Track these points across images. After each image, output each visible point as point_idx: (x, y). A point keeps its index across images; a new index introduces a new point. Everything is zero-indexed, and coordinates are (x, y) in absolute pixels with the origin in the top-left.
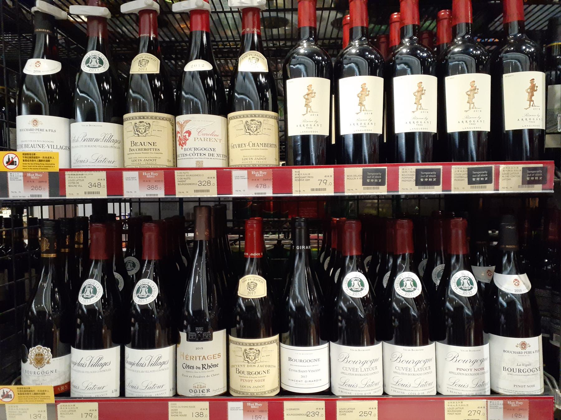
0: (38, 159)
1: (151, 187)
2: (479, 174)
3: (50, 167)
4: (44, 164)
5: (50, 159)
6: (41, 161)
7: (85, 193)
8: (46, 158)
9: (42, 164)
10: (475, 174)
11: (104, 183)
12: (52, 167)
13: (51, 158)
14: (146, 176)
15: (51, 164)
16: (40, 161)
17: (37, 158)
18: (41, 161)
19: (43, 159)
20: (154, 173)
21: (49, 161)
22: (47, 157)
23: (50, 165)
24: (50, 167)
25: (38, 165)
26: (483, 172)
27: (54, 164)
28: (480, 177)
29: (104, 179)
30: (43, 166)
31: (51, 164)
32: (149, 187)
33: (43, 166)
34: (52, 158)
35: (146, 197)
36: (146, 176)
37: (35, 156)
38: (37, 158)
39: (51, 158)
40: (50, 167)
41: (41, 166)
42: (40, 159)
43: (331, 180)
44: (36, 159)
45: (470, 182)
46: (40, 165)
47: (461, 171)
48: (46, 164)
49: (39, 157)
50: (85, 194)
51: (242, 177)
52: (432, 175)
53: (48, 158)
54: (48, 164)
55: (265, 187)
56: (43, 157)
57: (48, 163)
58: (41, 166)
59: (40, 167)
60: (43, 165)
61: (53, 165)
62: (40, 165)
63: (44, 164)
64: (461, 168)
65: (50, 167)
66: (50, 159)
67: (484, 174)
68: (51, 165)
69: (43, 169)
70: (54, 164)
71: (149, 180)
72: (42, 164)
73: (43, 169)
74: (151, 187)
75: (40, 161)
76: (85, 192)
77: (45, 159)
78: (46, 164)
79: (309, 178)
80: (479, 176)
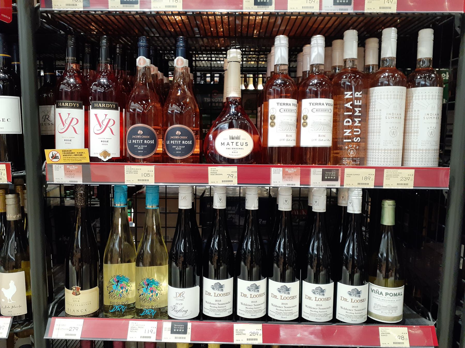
0: (74, 154)
5: (82, 154)
8: (79, 153)
12: (85, 159)
13: (83, 153)
16: (75, 155)
17: (73, 153)
19: (78, 154)
21: (82, 155)
22: (80, 152)
25: (74, 158)
37: (71, 152)
38: (73, 153)
39: (83, 153)
44: (72, 154)
49: (74, 153)
53: (81, 153)
56: (77, 153)
57: (81, 156)
60: (78, 158)
61: (85, 158)
62: (76, 158)
68: (84, 158)
75: (75, 155)
77: (79, 154)
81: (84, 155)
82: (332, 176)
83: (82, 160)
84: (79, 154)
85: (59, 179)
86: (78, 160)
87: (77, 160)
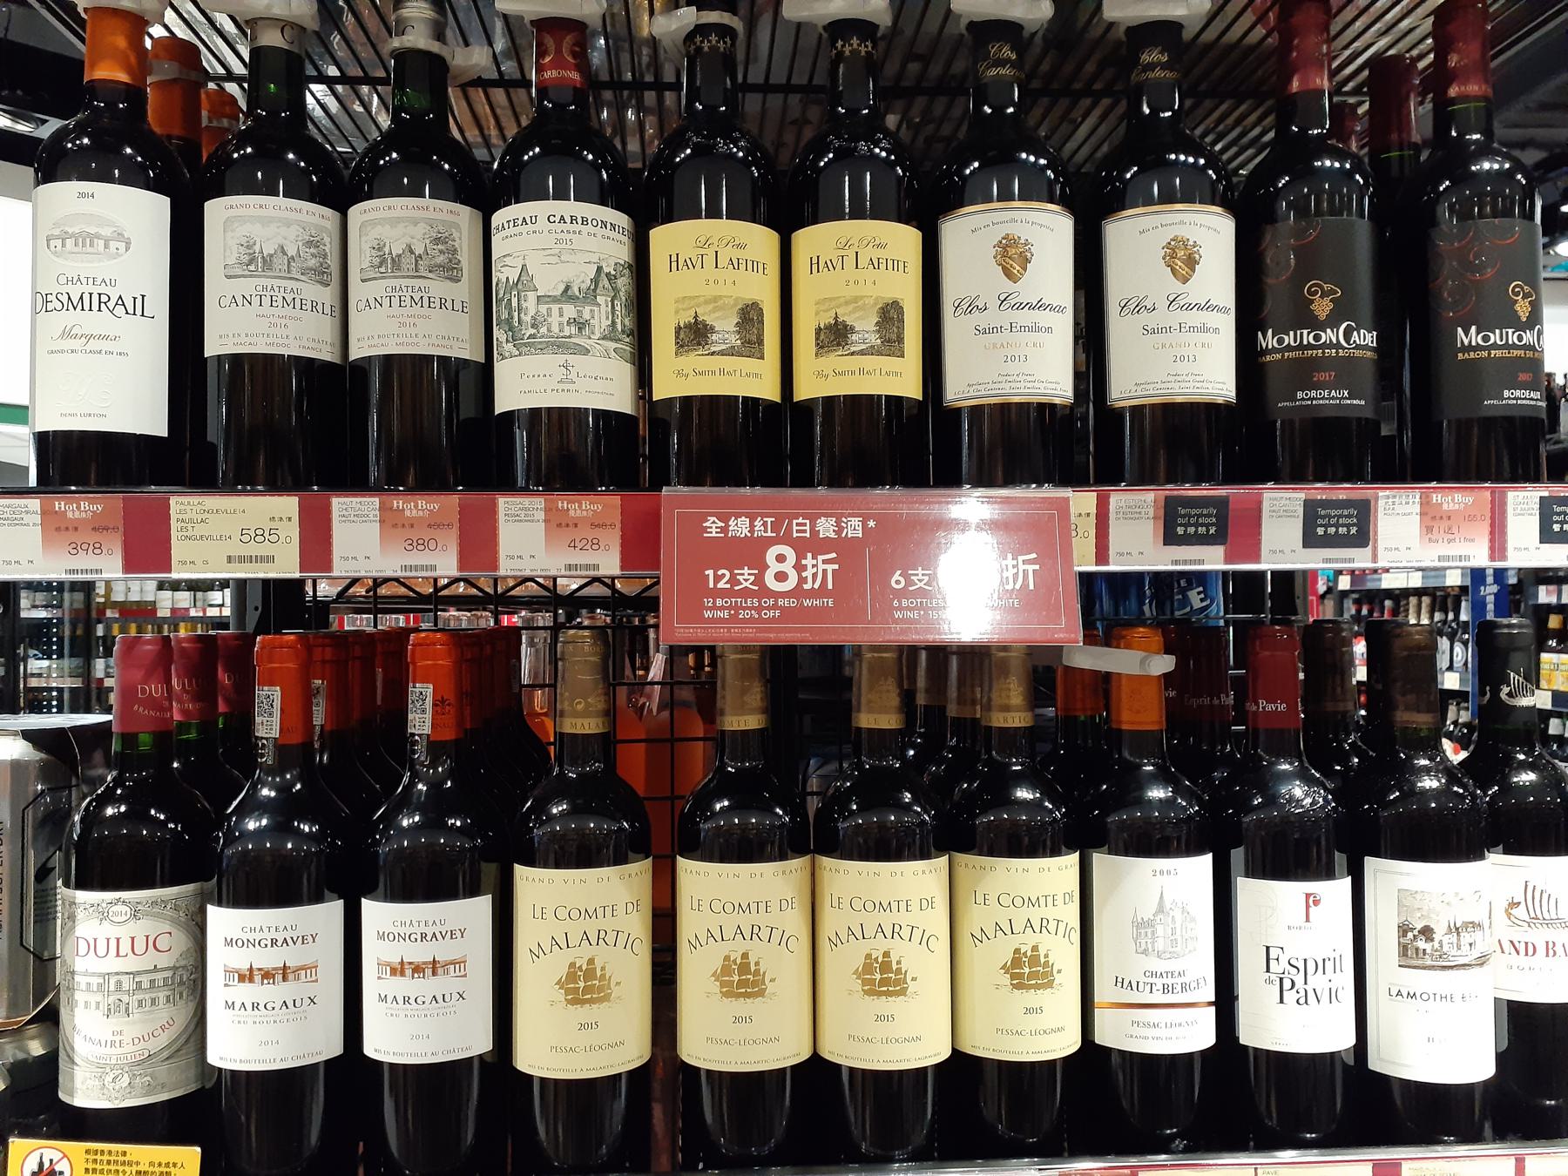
1: (415, 544)
2: (1334, 517)
7: (230, 560)
10: (1183, 516)
14: (403, 510)
26: (1346, 512)
28: (1197, 525)
32: (410, 542)
43: (292, 531)
45: (1170, 538)
52: (1205, 516)
55: (595, 547)
67: (1349, 516)
74: (415, 544)
79: (215, 526)
80: (1333, 521)
82: (1343, 525)
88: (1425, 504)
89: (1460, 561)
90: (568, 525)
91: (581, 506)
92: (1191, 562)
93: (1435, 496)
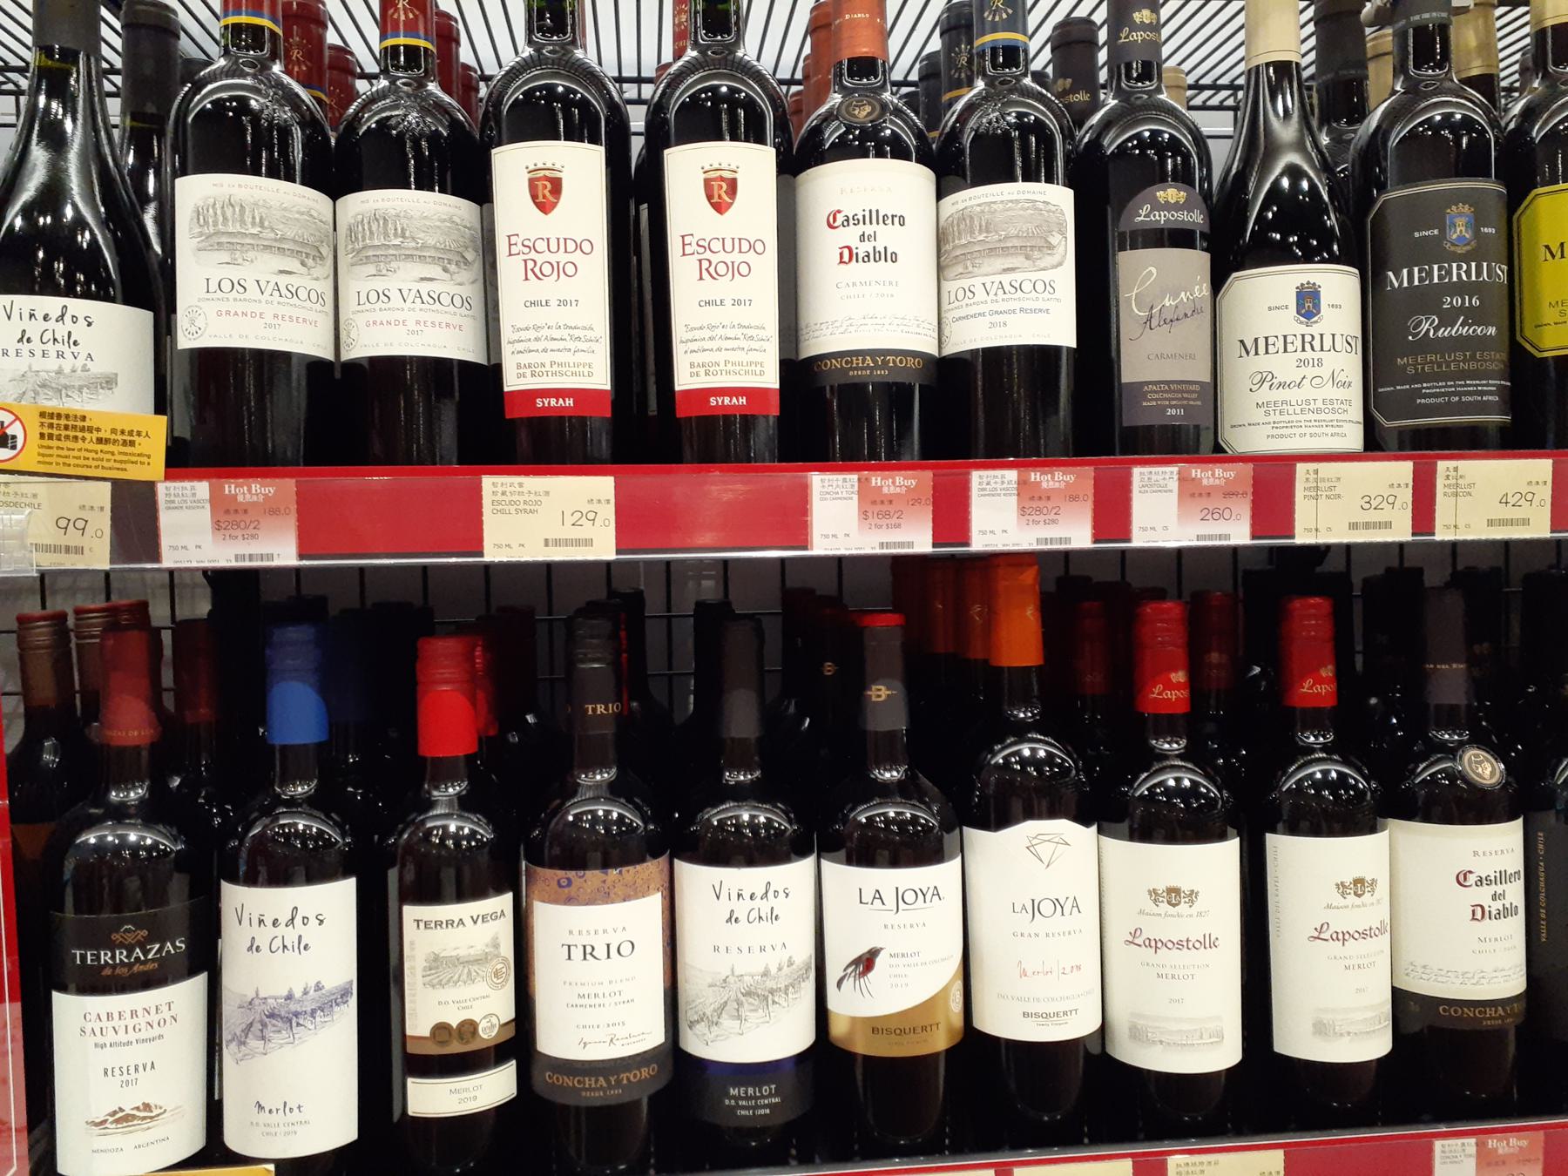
3: (133, 463)
4: (113, 454)
5: (136, 438)
6: (107, 441)
9: (107, 452)
11: (608, 513)
13: (139, 434)
15: (139, 455)
16: (100, 441)
18: (107, 441)
19: (113, 437)
20: (1224, 470)
21: (132, 443)
22: (127, 429)
23: (134, 459)
24: (136, 463)
27: (149, 457)
29: (608, 502)
30: (108, 460)
31: (139, 455)
33: (108, 460)
34: (144, 434)
35: (234, 564)
36: (1201, 479)
39: (139, 434)
40: (136, 463)
41: (102, 460)
42: (101, 435)
46: (100, 455)
47: (504, 493)
48: (120, 453)
49: (98, 430)
50: (547, 545)
51: (196, 504)
53: (131, 433)
54: (126, 454)
56: (114, 431)
57: (128, 449)
58: (102, 460)
59: (99, 463)
60: (109, 456)
61: (145, 459)
62: (100, 455)
63: (113, 454)
64: (521, 485)
65: (133, 463)
66: (136, 438)
68: (139, 459)
69: (110, 469)
70: (149, 457)
71: (1208, 493)
72: (107, 452)
73: (110, 469)
75: (100, 441)
76: (546, 540)
77: (120, 437)
78: (120, 453)
81: (143, 446)
83: (128, 466)
84: (120, 437)
85: (508, 546)
86: (111, 464)
87: (105, 464)
88: (1183, 480)
89: (1046, 544)
90: (1200, 495)
91: (251, 490)
92: (901, 545)
93: (1033, 474)
